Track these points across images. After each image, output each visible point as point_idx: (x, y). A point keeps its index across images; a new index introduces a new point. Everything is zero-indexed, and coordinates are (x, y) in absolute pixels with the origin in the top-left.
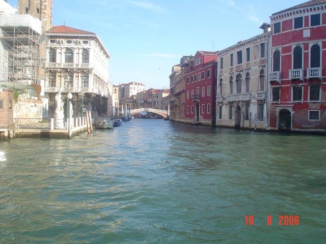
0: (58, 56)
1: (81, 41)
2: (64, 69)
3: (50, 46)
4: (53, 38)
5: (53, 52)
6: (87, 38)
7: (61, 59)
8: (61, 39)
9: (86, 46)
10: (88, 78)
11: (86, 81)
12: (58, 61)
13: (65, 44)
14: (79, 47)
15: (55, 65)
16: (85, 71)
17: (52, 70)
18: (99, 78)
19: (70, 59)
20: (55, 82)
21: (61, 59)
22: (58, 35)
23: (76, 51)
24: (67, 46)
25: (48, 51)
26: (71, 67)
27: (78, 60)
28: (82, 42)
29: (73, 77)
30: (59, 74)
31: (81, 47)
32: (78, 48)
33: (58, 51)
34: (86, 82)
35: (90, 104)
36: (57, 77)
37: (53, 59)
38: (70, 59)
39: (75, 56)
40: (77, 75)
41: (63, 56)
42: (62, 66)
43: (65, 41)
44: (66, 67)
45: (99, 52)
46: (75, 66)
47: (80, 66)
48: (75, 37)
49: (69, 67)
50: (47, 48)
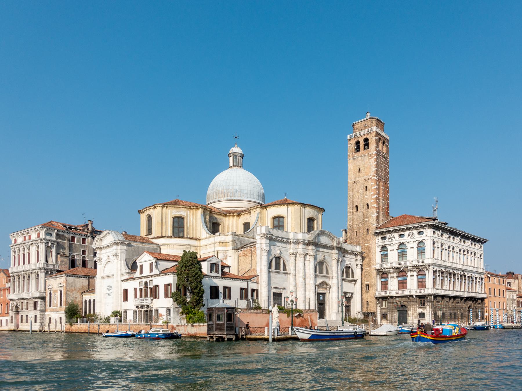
0: (390, 253)
2: (396, 268)
3: (381, 244)
4: (382, 235)
7: (393, 258)
8: (393, 234)
19: (402, 255)
21: (393, 258)
22: (388, 229)
23: (408, 246)
25: (379, 249)
29: (407, 276)
30: (392, 275)
33: (389, 248)
35: (428, 308)
36: (389, 278)
37: (384, 257)
38: (402, 255)
39: (409, 251)
40: (412, 273)
42: (394, 265)
43: (396, 235)
44: (399, 266)
47: (414, 263)
50: (378, 246)
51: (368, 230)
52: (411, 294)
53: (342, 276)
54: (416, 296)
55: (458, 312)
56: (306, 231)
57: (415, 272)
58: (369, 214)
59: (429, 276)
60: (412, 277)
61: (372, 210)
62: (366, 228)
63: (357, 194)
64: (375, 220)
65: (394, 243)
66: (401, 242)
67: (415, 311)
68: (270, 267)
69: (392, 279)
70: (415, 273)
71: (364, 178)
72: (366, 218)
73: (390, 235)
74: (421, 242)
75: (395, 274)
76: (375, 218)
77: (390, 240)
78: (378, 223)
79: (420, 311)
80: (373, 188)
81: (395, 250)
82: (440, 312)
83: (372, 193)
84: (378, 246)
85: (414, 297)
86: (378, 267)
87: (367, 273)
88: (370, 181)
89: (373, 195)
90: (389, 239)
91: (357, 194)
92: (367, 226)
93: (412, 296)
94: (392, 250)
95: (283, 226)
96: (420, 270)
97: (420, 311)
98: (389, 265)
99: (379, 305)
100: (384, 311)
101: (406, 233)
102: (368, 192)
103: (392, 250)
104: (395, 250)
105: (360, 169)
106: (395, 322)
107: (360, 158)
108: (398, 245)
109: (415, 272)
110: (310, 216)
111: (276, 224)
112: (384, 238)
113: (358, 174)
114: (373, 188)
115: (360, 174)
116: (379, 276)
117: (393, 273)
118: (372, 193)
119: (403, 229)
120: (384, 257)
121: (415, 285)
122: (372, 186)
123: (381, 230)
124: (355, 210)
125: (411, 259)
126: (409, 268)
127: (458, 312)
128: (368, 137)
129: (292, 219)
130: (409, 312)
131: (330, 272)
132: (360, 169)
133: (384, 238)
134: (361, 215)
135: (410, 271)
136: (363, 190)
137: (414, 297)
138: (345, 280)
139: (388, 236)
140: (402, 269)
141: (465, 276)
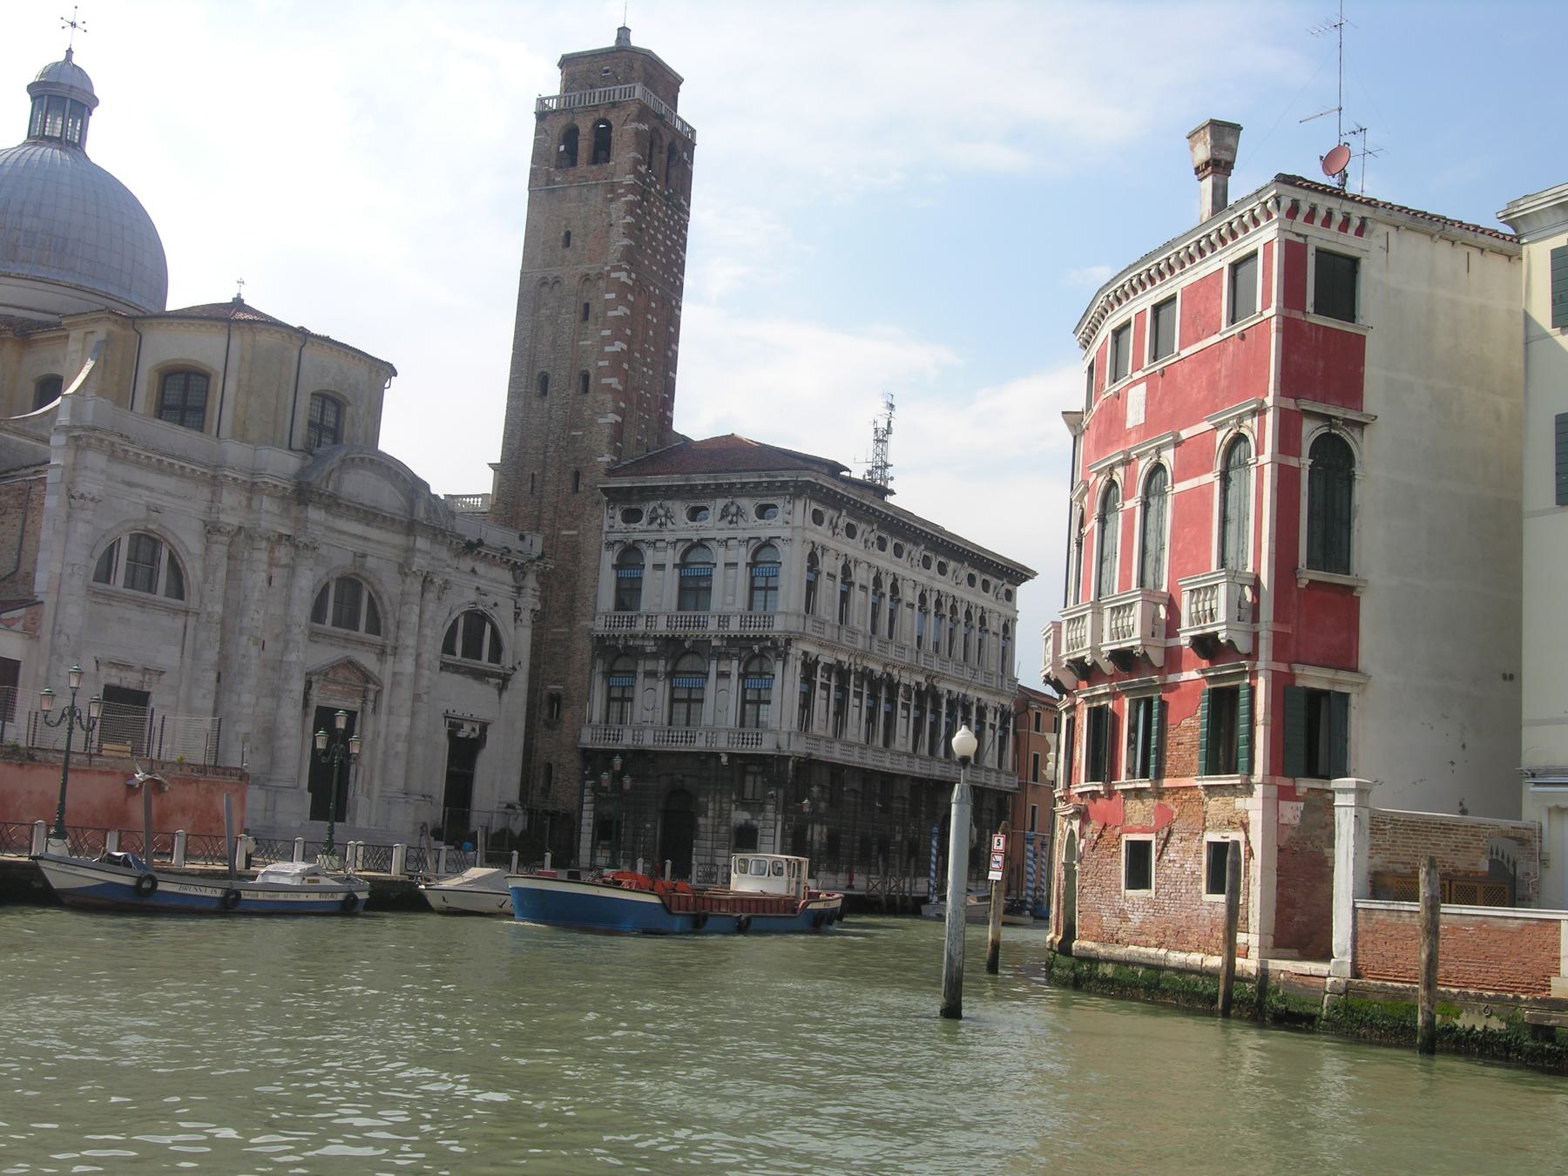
1: (749, 505)
4: (630, 504)
5: (630, 556)
6: (771, 488)
8: (668, 503)
9: (765, 529)
10: (765, 675)
13: (682, 526)
15: (631, 622)
16: (756, 648)
18: (881, 687)
19: (694, 589)
23: (720, 556)
25: (609, 558)
26: (698, 632)
28: (753, 510)
29: (707, 675)
30: (650, 665)
31: (747, 535)
32: (727, 535)
33: (650, 557)
34: (753, 701)
35: (769, 807)
36: (640, 677)
37: (628, 595)
42: (661, 627)
43: (679, 509)
44: (679, 632)
45: (885, 561)
46: (713, 625)
47: (734, 627)
48: (719, 491)
50: (610, 545)
51: (577, 475)
52: (714, 748)
53: (448, 648)
54: (731, 756)
55: (899, 838)
56: (298, 443)
59: (786, 684)
60: (723, 683)
61: (601, 397)
65: (669, 537)
66: (695, 538)
67: (723, 816)
68: (104, 572)
69: (649, 682)
70: (734, 667)
71: (583, 268)
72: (577, 428)
73: (652, 505)
74: (768, 544)
77: (655, 526)
78: (618, 452)
79: (741, 817)
80: (611, 314)
81: (669, 567)
82: (817, 828)
83: (607, 333)
84: (610, 545)
85: (724, 759)
86: (600, 627)
88: (601, 284)
89: (610, 341)
93: (717, 756)
94: (659, 567)
95: (202, 410)
96: (755, 656)
97: (741, 817)
98: (641, 626)
99: (589, 783)
103: (659, 567)
104: (669, 567)
105: (568, 234)
107: (573, 192)
108: (681, 547)
109: (735, 663)
110: (326, 384)
111: (173, 397)
112: (632, 516)
114: (611, 314)
115: (567, 252)
116: (600, 666)
117: (655, 656)
118: (607, 333)
119: (705, 486)
121: (731, 718)
122: (609, 305)
123: (625, 483)
125: (727, 609)
127: (899, 838)
129: (239, 386)
130: (701, 821)
131: (389, 623)
132: (568, 234)
133: (632, 516)
135: (720, 655)
137: (724, 759)
138: (456, 669)
139: (647, 508)
140: (687, 645)
141: (936, 698)
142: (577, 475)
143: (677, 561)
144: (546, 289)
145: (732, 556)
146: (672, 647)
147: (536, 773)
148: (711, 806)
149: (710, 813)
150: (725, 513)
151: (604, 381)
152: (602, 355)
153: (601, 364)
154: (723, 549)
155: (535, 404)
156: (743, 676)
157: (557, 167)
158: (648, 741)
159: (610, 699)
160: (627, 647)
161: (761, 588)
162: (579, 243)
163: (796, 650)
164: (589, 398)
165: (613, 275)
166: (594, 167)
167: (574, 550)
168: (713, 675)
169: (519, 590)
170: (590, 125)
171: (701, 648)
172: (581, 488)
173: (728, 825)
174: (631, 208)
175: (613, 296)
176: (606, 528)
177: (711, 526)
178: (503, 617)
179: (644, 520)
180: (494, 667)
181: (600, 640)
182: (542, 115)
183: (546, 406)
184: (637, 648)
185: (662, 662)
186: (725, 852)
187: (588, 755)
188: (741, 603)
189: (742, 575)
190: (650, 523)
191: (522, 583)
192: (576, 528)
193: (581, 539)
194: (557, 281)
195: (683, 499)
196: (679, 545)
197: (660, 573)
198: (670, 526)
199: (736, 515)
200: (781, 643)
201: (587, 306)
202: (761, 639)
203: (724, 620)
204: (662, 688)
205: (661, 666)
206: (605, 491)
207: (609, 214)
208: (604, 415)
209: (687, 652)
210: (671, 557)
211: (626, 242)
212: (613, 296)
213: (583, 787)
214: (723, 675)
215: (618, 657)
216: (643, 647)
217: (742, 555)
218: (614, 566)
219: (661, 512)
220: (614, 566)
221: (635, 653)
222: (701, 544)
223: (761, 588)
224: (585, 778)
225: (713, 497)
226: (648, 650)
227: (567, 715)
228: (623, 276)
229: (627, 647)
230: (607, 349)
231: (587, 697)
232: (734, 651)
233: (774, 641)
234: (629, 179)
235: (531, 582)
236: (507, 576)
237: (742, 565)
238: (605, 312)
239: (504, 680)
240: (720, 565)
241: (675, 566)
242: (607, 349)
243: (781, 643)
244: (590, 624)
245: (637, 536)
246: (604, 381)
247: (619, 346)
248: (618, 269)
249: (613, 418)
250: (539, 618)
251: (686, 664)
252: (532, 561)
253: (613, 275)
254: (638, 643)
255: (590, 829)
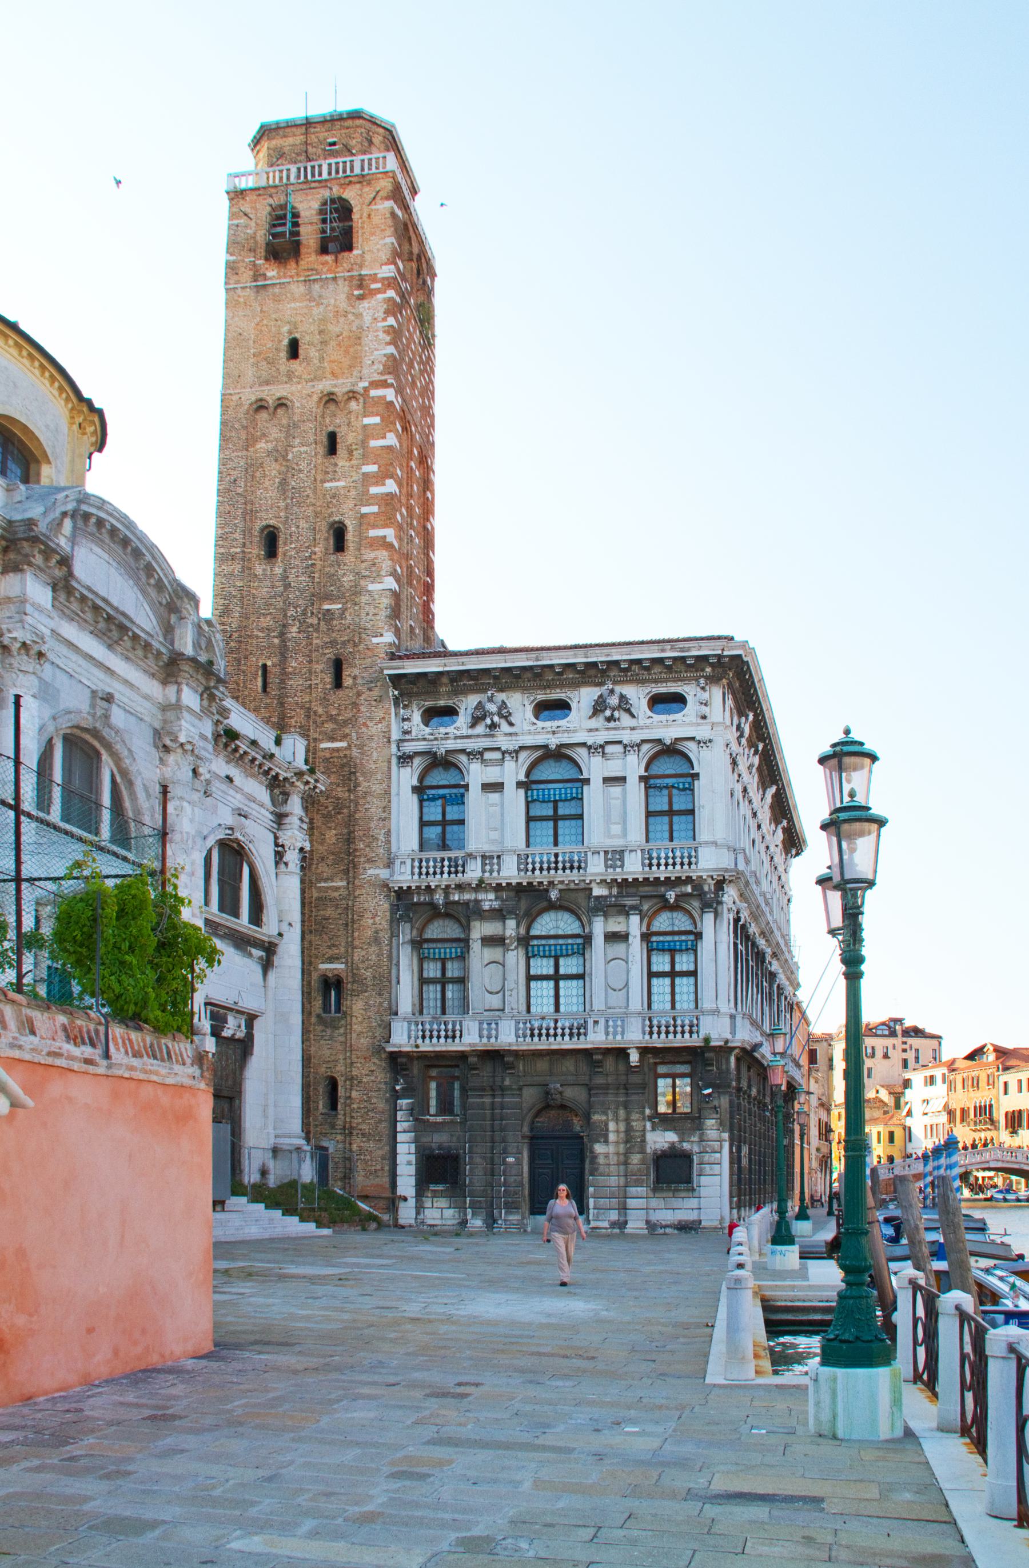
1: (638, 695)
2: (519, 890)
3: (420, 746)
7: (496, 826)
8: (501, 696)
11: (684, 963)
12: (478, 836)
13: (526, 726)
14: (627, 737)
15: (456, 867)
16: (671, 896)
17: (439, 898)
20: (462, 981)
21: (496, 826)
23: (595, 768)
24: (540, 740)
25: (407, 778)
26: (574, 876)
27: (614, 824)
28: (644, 703)
29: (588, 939)
30: (491, 928)
31: (637, 737)
33: (476, 774)
36: (476, 946)
37: (443, 829)
39: (594, 795)
40: (616, 925)
41: (515, 800)
42: (510, 872)
43: (520, 705)
44: (539, 877)
46: (596, 867)
47: (633, 867)
49: (559, 876)
50: (405, 759)
52: (617, 1041)
57: (635, 919)
58: (347, 580)
60: (619, 949)
61: (369, 555)
62: (330, 653)
63: (273, 469)
64: (383, 614)
66: (553, 742)
67: (632, 1141)
69: (495, 953)
70: (634, 925)
71: (326, 385)
72: (329, 598)
75: (511, 923)
76: (386, 601)
77: (480, 729)
80: (374, 443)
81: (510, 787)
83: (373, 468)
85: (634, 1057)
86: (404, 877)
87: (329, 912)
88: (353, 405)
89: (379, 479)
90: (475, 721)
91: (273, 469)
92: (333, 643)
94: (495, 787)
96: (667, 906)
97: (660, 1139)
98: (474, 872)
99: (403, 1102)
100: (439, 1139)
101: (584, 698)
102: (341, 460)
103: (495, 787)
106: (511, 1207)
109: (635, 919)
113: (283, 362)
114: (374, 443)
115: (295, 365)
117: (499, 915)
118: (373, 468)
120: (443, 829)
124: (256, 550)
125: (617, 843)
126: (597, 891)
128: (350, 194)
130: (599, 1148)
134: (299, 579)
135: (604, 908)
136: (306, 451)
137: (634, 1057)
139: (468, 703)
140: (554, 895)
142: (338, 666)
143: (522, 777)
144: (264, 415)
145: (614, 768)
146: (528, 899)
147: (323, 1094)
148: (612, 1126)
149: (612, 1137)
150: (599, 707)
151: (373, 533)
152: (365, 498)
153: (365, 510)
154: (597, 760)
155: (259, 570)
156: (646, 937)
157: (267, 259)
158: (507, 1037)
159: (423, 981)
160: (448, 903)
161: (661, 813)
162: (313, 353)
163: (730, 895)
164: (349, 557)
165: (373, 393)
166: (329, 258)
167: (347, 770)
168: (598, 940)
169: (280, 818)
170: (316, 205)
171: (576, 901)
172: (347, 681)
173: (643, 1151)
174: (393, 309)
175: (377, 420)
176: (395, 735)
177: (578, 725)
178: (262, 853)
179: (462, 721)
180: (252, 930)
181: (402, 894)
182: (236, 195)
183: (278, 570)
184: (467, 904)
185: (511, 923)
186: (641, 1190)
187: (398, 1062)
188: (636, 834)
189: (635, 791)
190: (473, 726)
191: (286, 809)
192: (345, 737)
193: (355, 752)
194: (281, 404)
195: (524, 689)
196: (523, 755)
197: (494, 797)
198: (505, 727)
199: (619, 707)
200: (709, 886)
201: (332, 438)
202: (679, 881)
203: (615, 856)
204: (515, 958)
205: (511, 928)
206: (397, 680)
207: (359, 316)
208: (377, 578)
209: (552, 907)
210: (513, 772)
211: (391, 349)
212: (377, 420)
213: (395, 1110)
214: (612, 937)
215: (436, 918)
216: (477, 902)
217: (634, 766)
218: (416, 790)
219: (492, 708)
220: (416, 790)
221: (464, 914)
222: (558, 754)
223: (661, 813)
224: (396, 1096)
225: (575, 685)
226: (486, 906)
227: (357, 1006)
228: (390, 394)
229: (448, 903)
230: (374, 490)
231: (386, 983)
232: (629, 902)
233: (697, 884)
234: (388, 271)
235: (295, 806)
236: (263, 795)
237: (633, 780)
238: (364, 443)
239: (270, 949)
240: (596, 782)
241: (520, 784)
242: (374, 490)
243: (709, 886)
244: (384, 873)
245: (451, 744)
246: (373, 533)
247: (390, 486)
248: (384, 384)
249: (390, 583)
250: (306, 859)
251: (548, 924)
252: (300, 774)
253: (373, 393)
254: (467, 896)
255: (412, 1170)
